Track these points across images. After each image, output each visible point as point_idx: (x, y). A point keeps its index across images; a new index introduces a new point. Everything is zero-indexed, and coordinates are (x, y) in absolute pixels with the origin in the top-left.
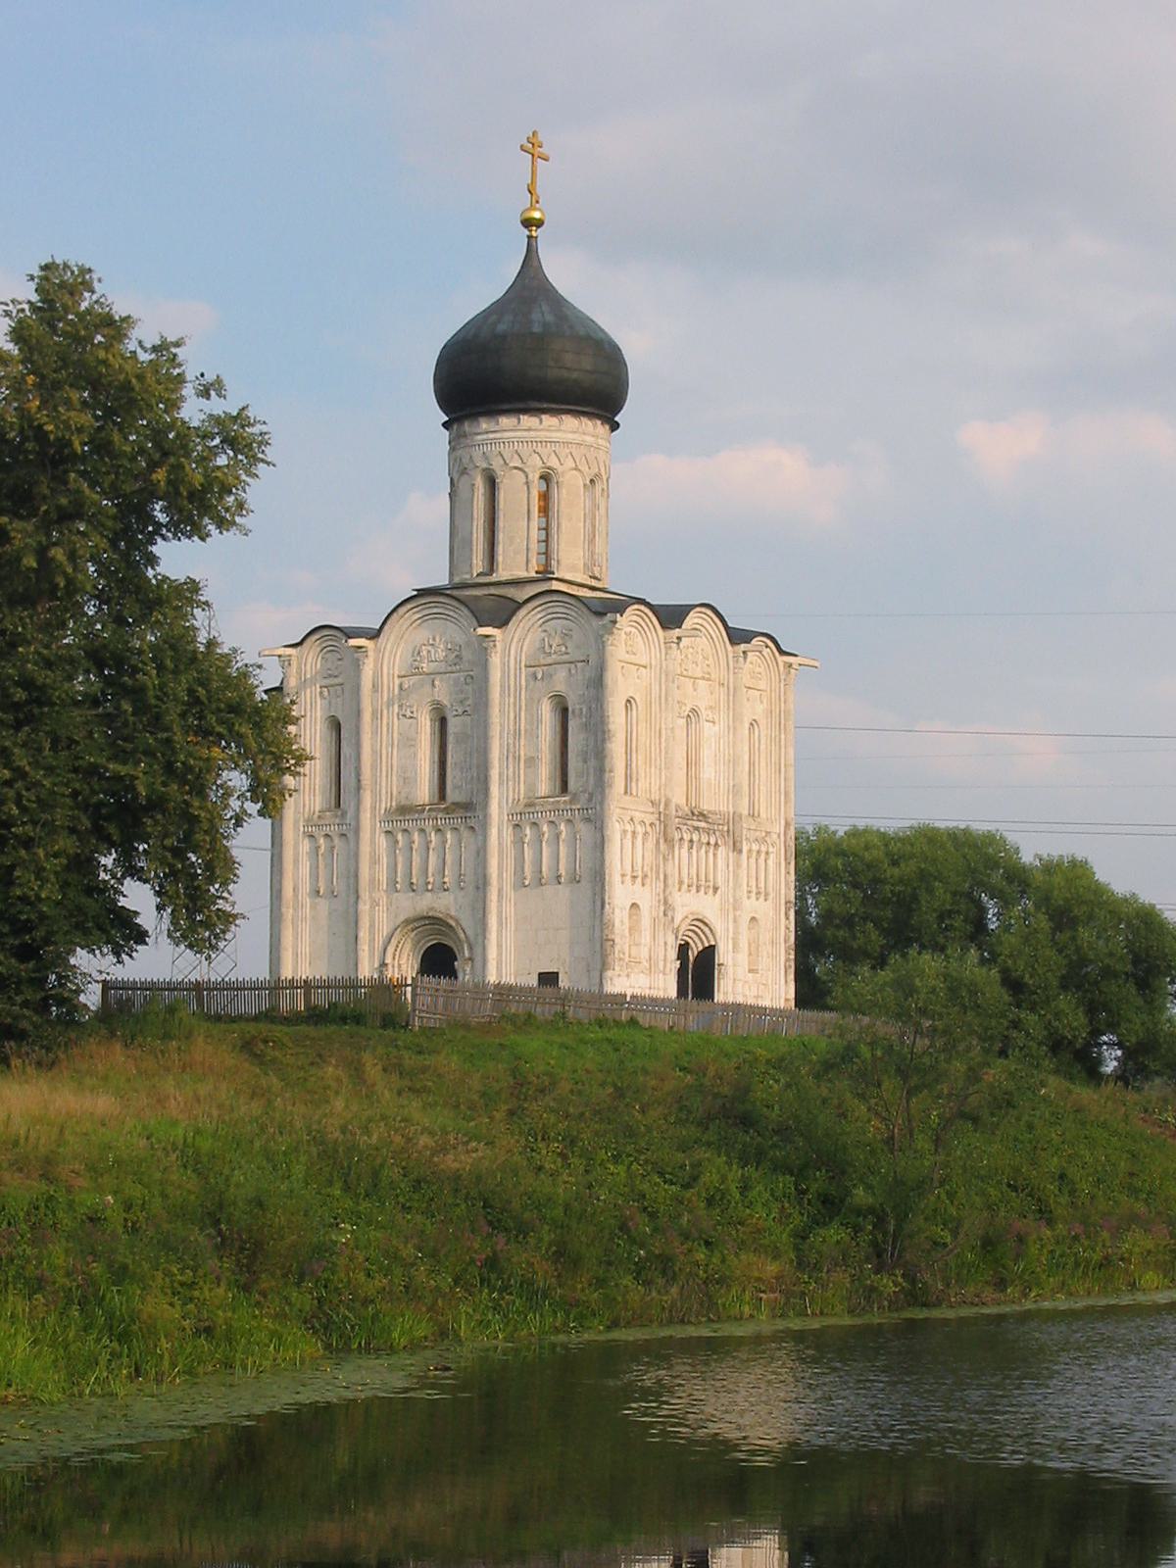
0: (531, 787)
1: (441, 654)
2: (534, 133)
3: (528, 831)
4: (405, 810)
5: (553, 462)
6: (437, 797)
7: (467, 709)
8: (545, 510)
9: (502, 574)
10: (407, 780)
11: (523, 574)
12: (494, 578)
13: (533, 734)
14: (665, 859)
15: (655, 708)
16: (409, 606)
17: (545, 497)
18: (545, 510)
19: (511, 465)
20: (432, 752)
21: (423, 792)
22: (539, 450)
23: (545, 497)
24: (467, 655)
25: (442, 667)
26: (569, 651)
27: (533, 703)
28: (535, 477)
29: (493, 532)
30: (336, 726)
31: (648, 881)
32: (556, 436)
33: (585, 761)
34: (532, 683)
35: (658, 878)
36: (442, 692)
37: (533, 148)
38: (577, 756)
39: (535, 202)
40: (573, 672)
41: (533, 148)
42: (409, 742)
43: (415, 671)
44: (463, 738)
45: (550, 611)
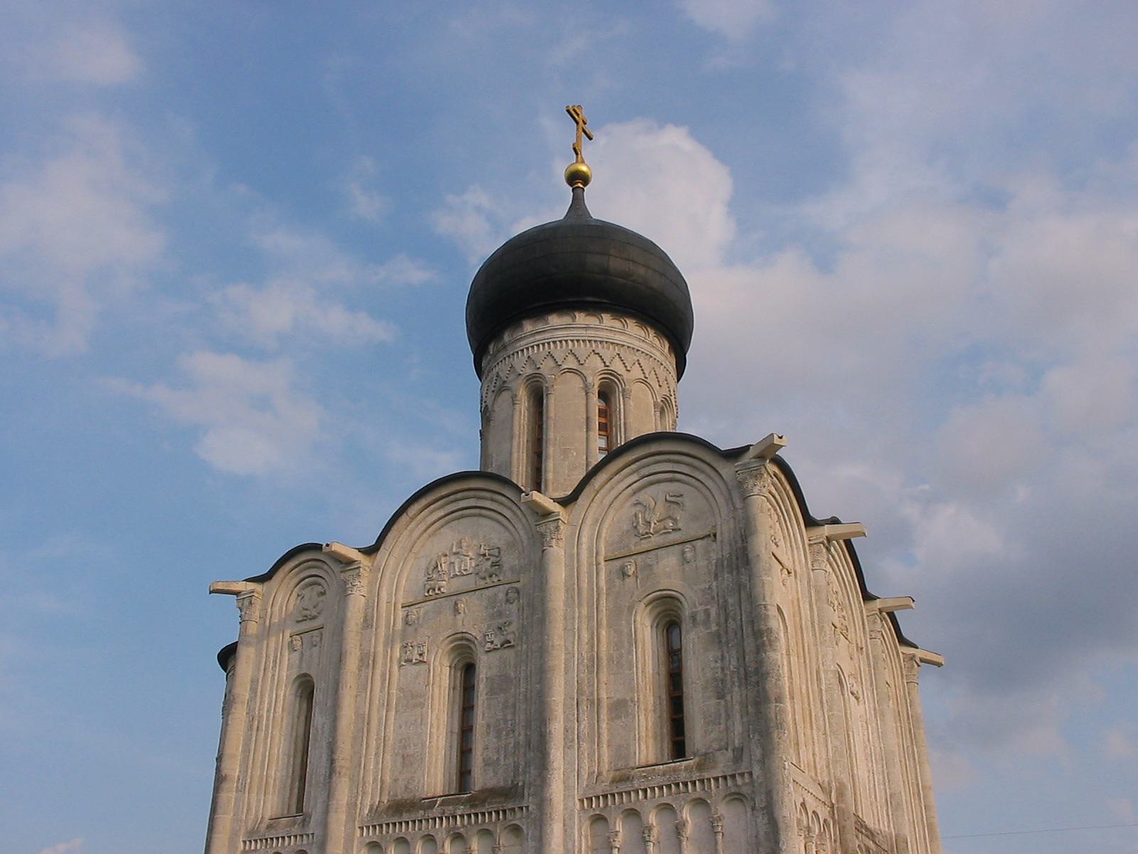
0: (621, 751)
1: (470, 565)
3: (619, 826)
4: (402, 808)
6: (454, 784)
7: (510, 637)
10: (408, 760)
13: (621, 663)
15: (808, 636)
16: (423, 502)
19: (564, 366)
20: (451, 716)
21: (435, 776)
22: (599, 349)
24: (509, 560)
25: (470, 583)
26: (680, 525)
27: (621, 612)
28: (595, 382)
29: (541, 414)
30: (306, 688)
32: (619, 338)
33: (721, 696)
34: (618, 582)
36: (473, 618)
38: (705, 688)
40: (689, 555)
42: (414, 700)
43: (431, 594)
44: (501, 684)
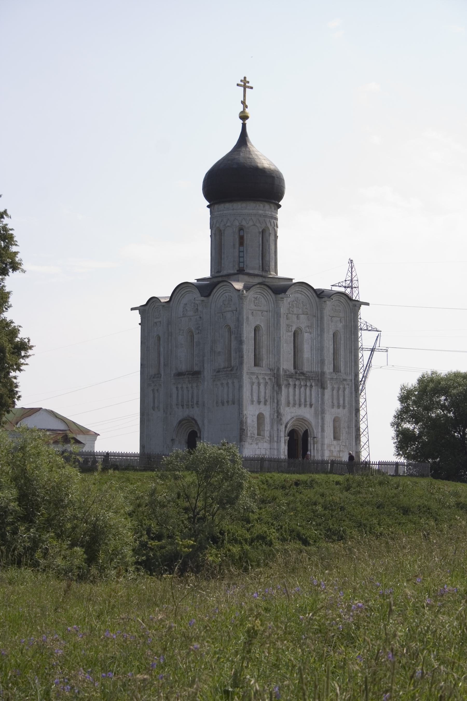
2: (245, 78)
5: (244, 223)
8: (241, 243)
9: (224, 272)
11: (232, 272)
12: (221, 274)
14: (277, 394)
17: (241, 238)
18: (241, 243)
23: (241, 238)
31: (268, 403)
35: (274, 402)
37: (245, 84)
39: (245, 106)
41: (245, 84)
45: (224, 289)
